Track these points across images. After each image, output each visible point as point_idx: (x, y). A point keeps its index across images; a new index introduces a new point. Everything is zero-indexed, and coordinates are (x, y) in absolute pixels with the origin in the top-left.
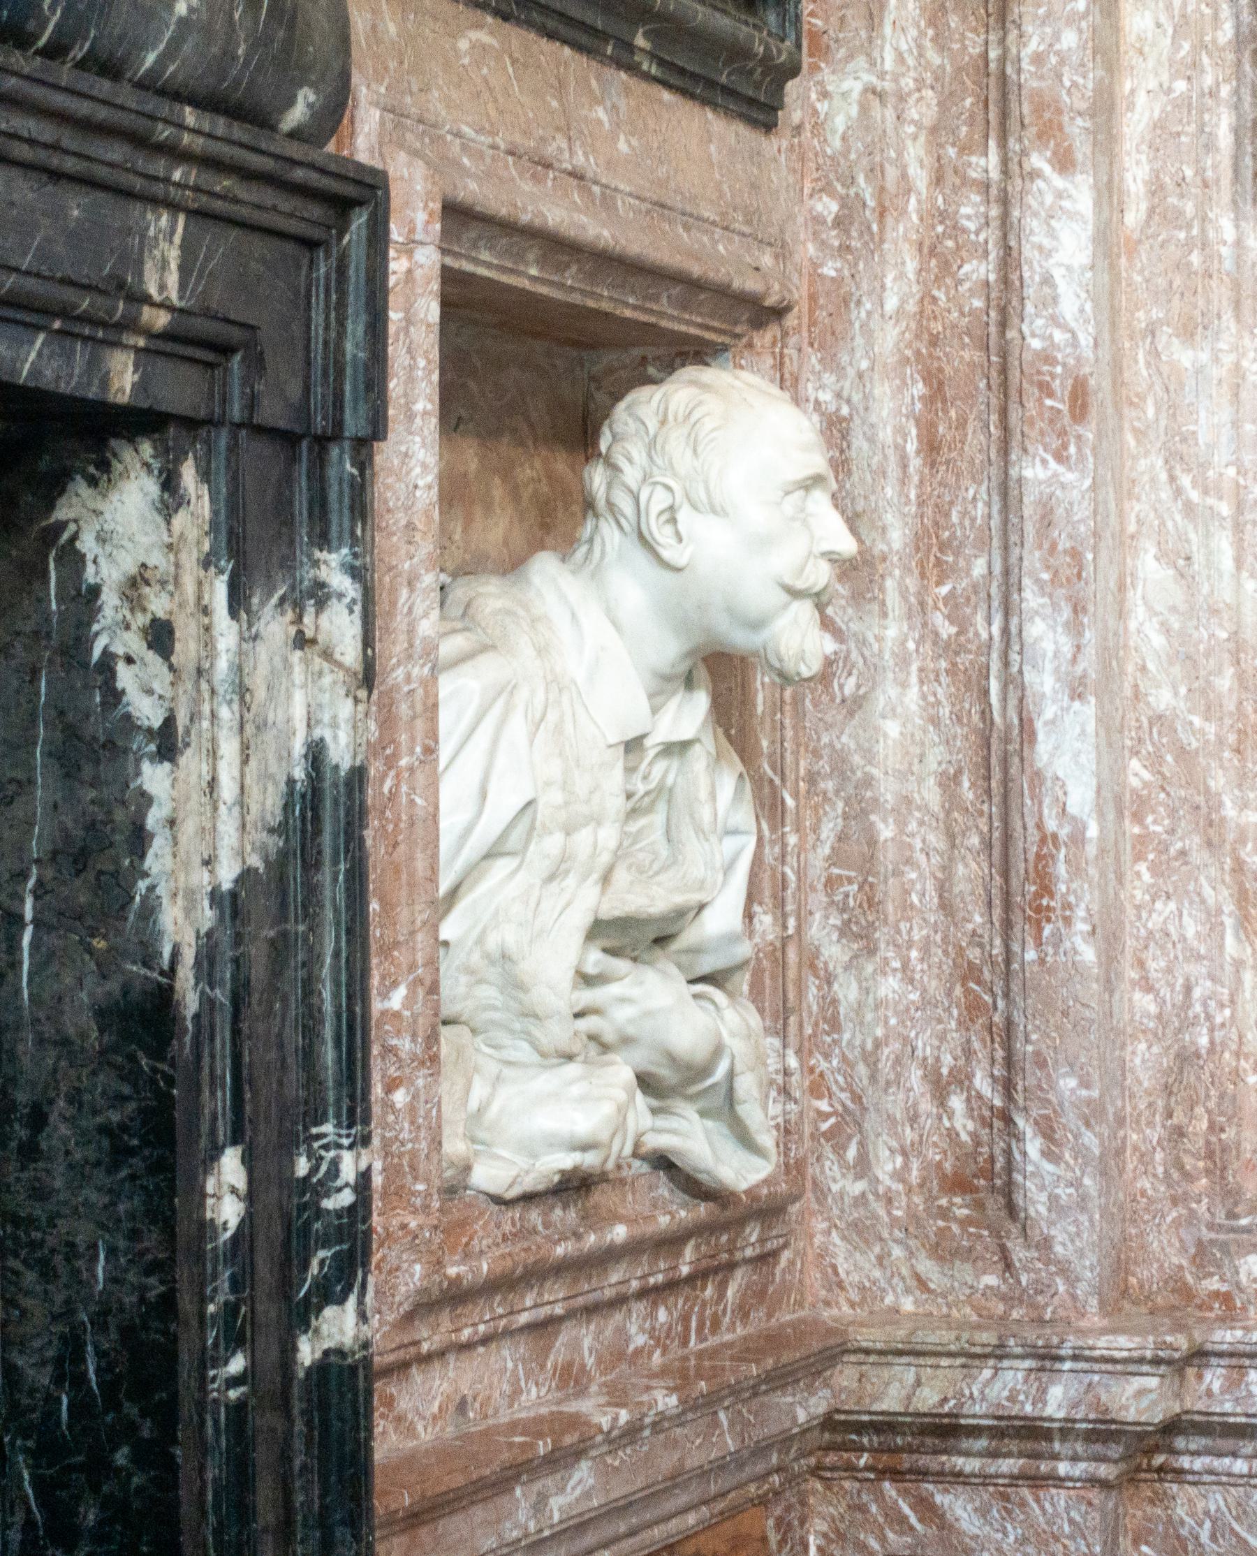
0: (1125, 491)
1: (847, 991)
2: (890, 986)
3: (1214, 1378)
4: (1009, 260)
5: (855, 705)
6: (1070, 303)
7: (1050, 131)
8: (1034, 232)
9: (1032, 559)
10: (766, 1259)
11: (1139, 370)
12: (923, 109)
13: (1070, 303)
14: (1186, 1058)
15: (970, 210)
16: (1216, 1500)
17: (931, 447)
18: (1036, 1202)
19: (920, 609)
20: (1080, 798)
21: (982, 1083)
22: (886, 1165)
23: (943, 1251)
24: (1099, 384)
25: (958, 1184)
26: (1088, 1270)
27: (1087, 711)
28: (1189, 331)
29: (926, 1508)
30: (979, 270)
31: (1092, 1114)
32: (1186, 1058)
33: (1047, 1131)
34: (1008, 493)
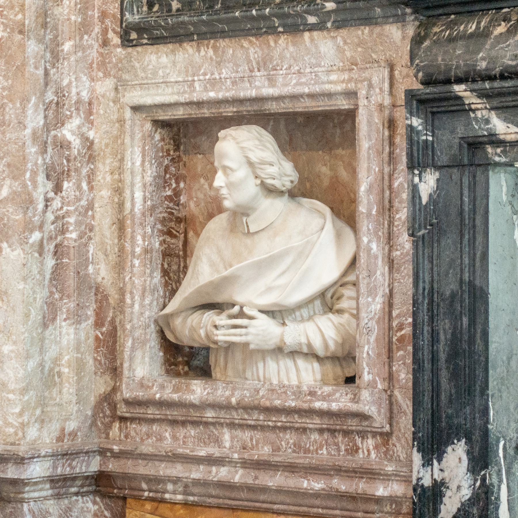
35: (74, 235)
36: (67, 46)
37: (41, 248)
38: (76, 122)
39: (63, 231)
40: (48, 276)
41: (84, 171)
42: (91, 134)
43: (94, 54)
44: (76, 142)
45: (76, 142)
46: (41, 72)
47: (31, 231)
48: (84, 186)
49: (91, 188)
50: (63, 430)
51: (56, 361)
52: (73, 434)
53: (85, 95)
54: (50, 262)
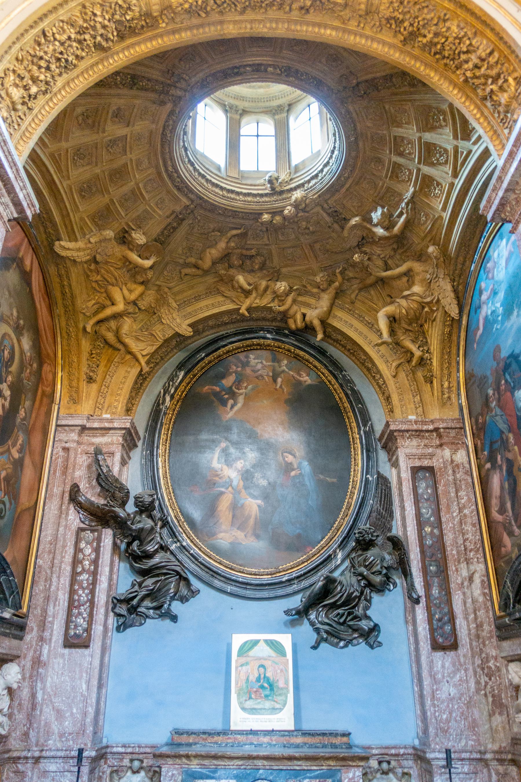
0: (48, 672)
1: (17, 717)
2: (21, 716)
3: (44, 752)
4: (41, 652)
5: (22, 691)
6: (45, 656)
7: (45, 642)
8: (43, 650)
9: (39, 678)
10: (5, 742)
11: (51, 661)
12: (35, 639)
13: (45, 656)
14: (46, 723)
15: (38, 647)
16: (43, 764)
17: (32, 668)
18: (31, 736)
19: (29, 682)
20: (40, 699)
21: (28, 725)
22: (18, 733)
23: (22, 741)
24: (47, 663)
25: (24, 735)
26: (34, 742)
27: (42, 691)
28: (55, 658)
29: (17, 766)
30: (38, 653)
31: (37, 728)
32: (46, 723)
33: (33, 729)
34: (38, 672)
35: (496, 692)
36: (487, 642)
37: (486, 695)
38: (492, 662)
39: (494, 690)
40: (490, 703)
41: (497, 674)
42: (498, 665)
43: (495, 644)
44: (493, 667)
45: (493, 667)
46: (478, 650)
47: (481, 690)
48: (498, 678)
49: (500, 679)
50: (501, 746)
51: (497, 726)
52: (505, 748)
53: (494, 654)
54: (490, 699)
